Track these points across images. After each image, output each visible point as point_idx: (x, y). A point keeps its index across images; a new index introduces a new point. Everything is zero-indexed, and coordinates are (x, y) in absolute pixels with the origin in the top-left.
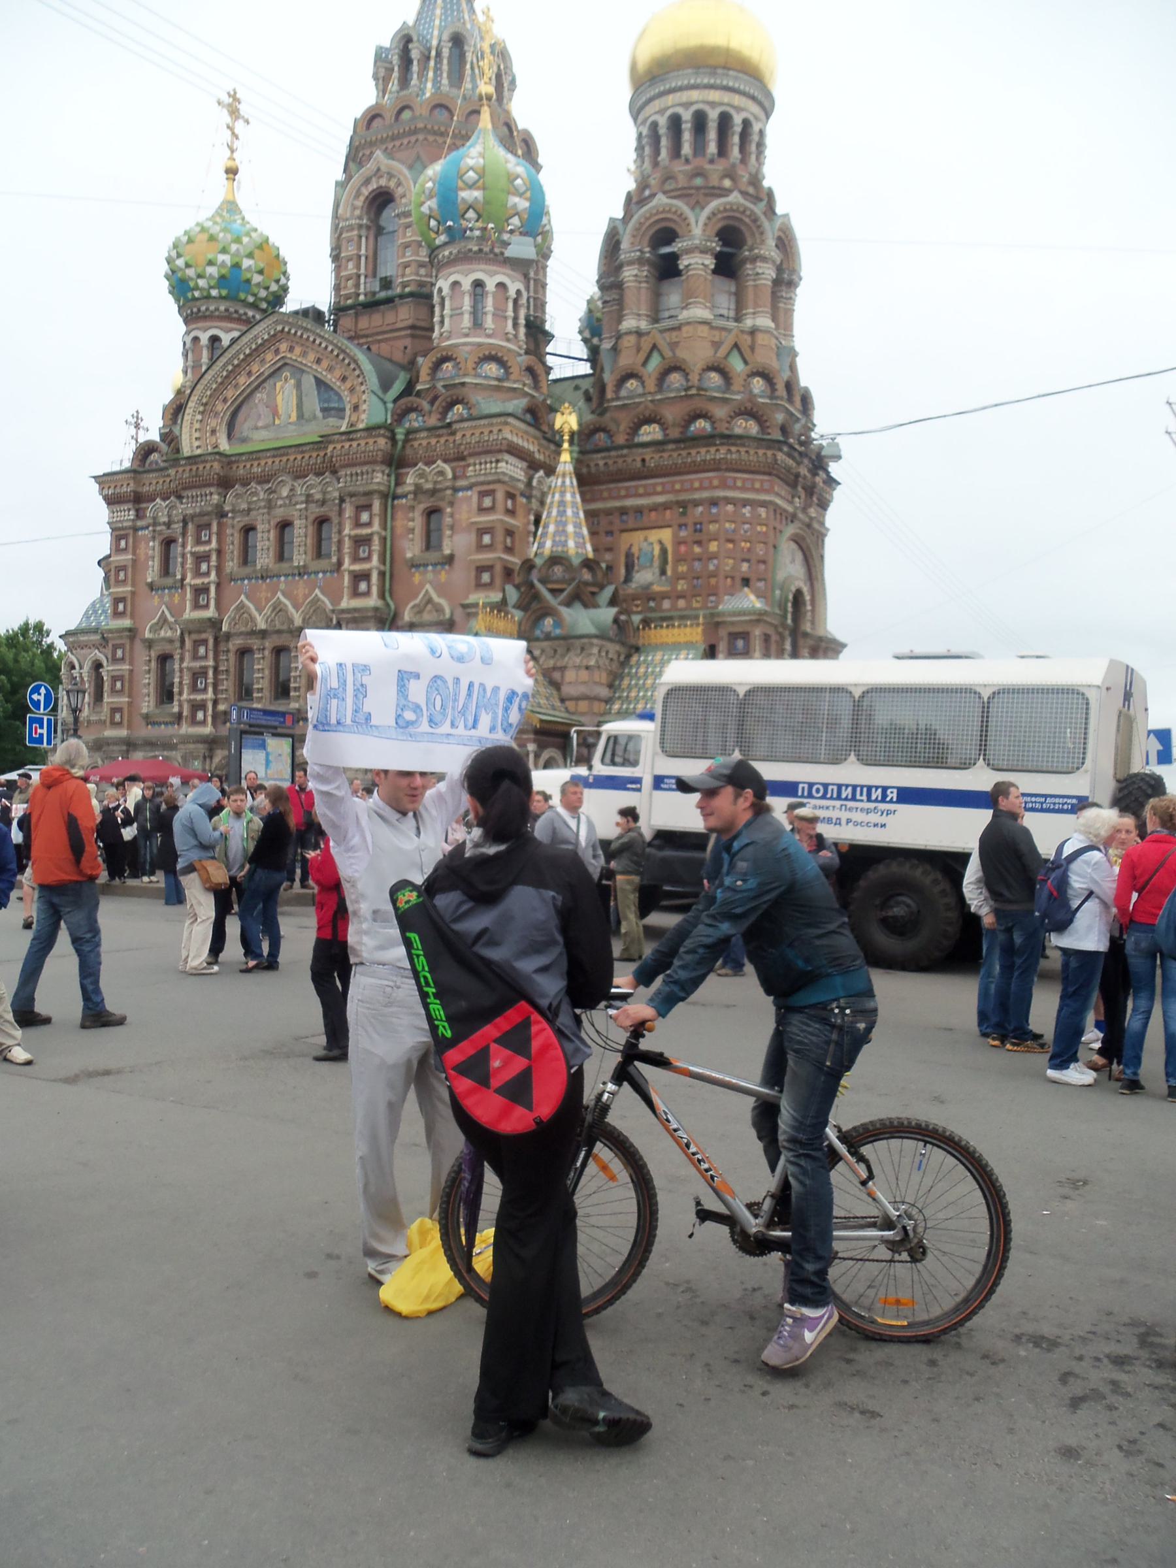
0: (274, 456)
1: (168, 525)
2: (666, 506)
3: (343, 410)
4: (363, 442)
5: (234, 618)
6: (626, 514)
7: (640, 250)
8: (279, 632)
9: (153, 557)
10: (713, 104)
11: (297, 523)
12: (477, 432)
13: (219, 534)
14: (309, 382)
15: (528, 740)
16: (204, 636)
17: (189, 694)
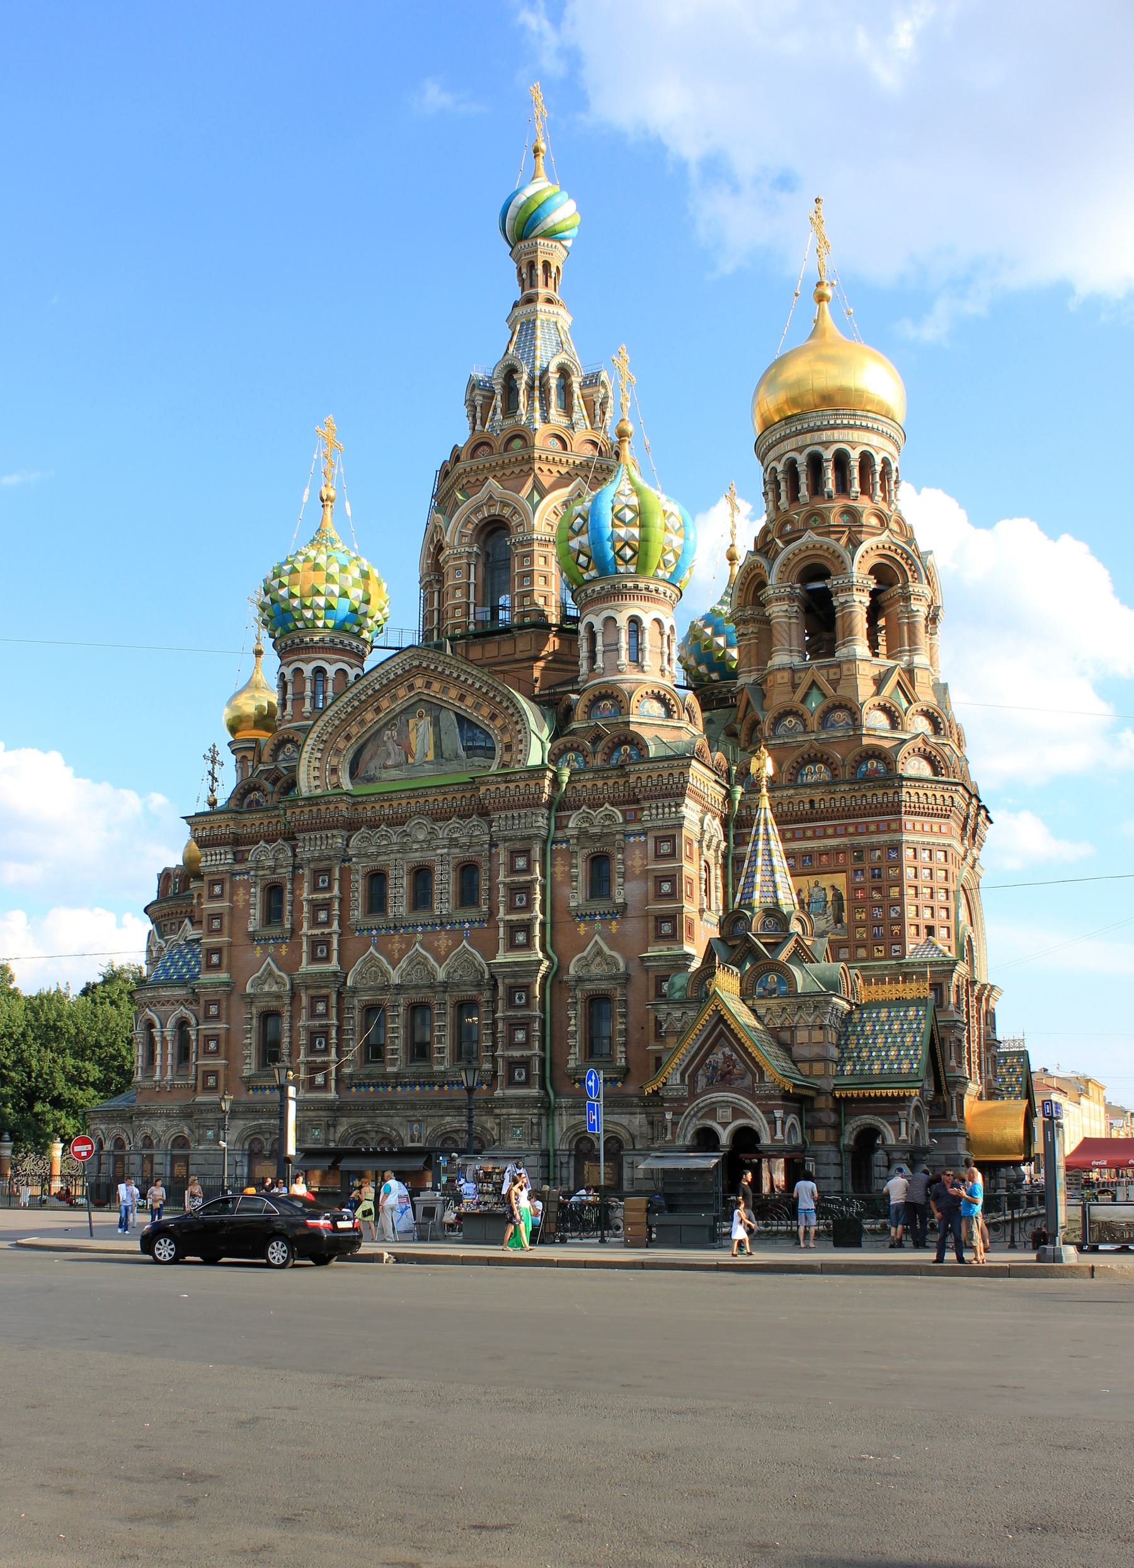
0: (409, 797)
1: (273, 870)
2: (837, 851)
3: (493, 749)
4: (522, 784)
5: (360, 973)
6: (793, 857)
7: (790, 586)
8: (416, 987)
11: (438, 869)
12: (654, 775)
13: (341, 880)
14: (448, 720)
15: (777, 1107)
16: (324, 991)
17: (307, 1055)
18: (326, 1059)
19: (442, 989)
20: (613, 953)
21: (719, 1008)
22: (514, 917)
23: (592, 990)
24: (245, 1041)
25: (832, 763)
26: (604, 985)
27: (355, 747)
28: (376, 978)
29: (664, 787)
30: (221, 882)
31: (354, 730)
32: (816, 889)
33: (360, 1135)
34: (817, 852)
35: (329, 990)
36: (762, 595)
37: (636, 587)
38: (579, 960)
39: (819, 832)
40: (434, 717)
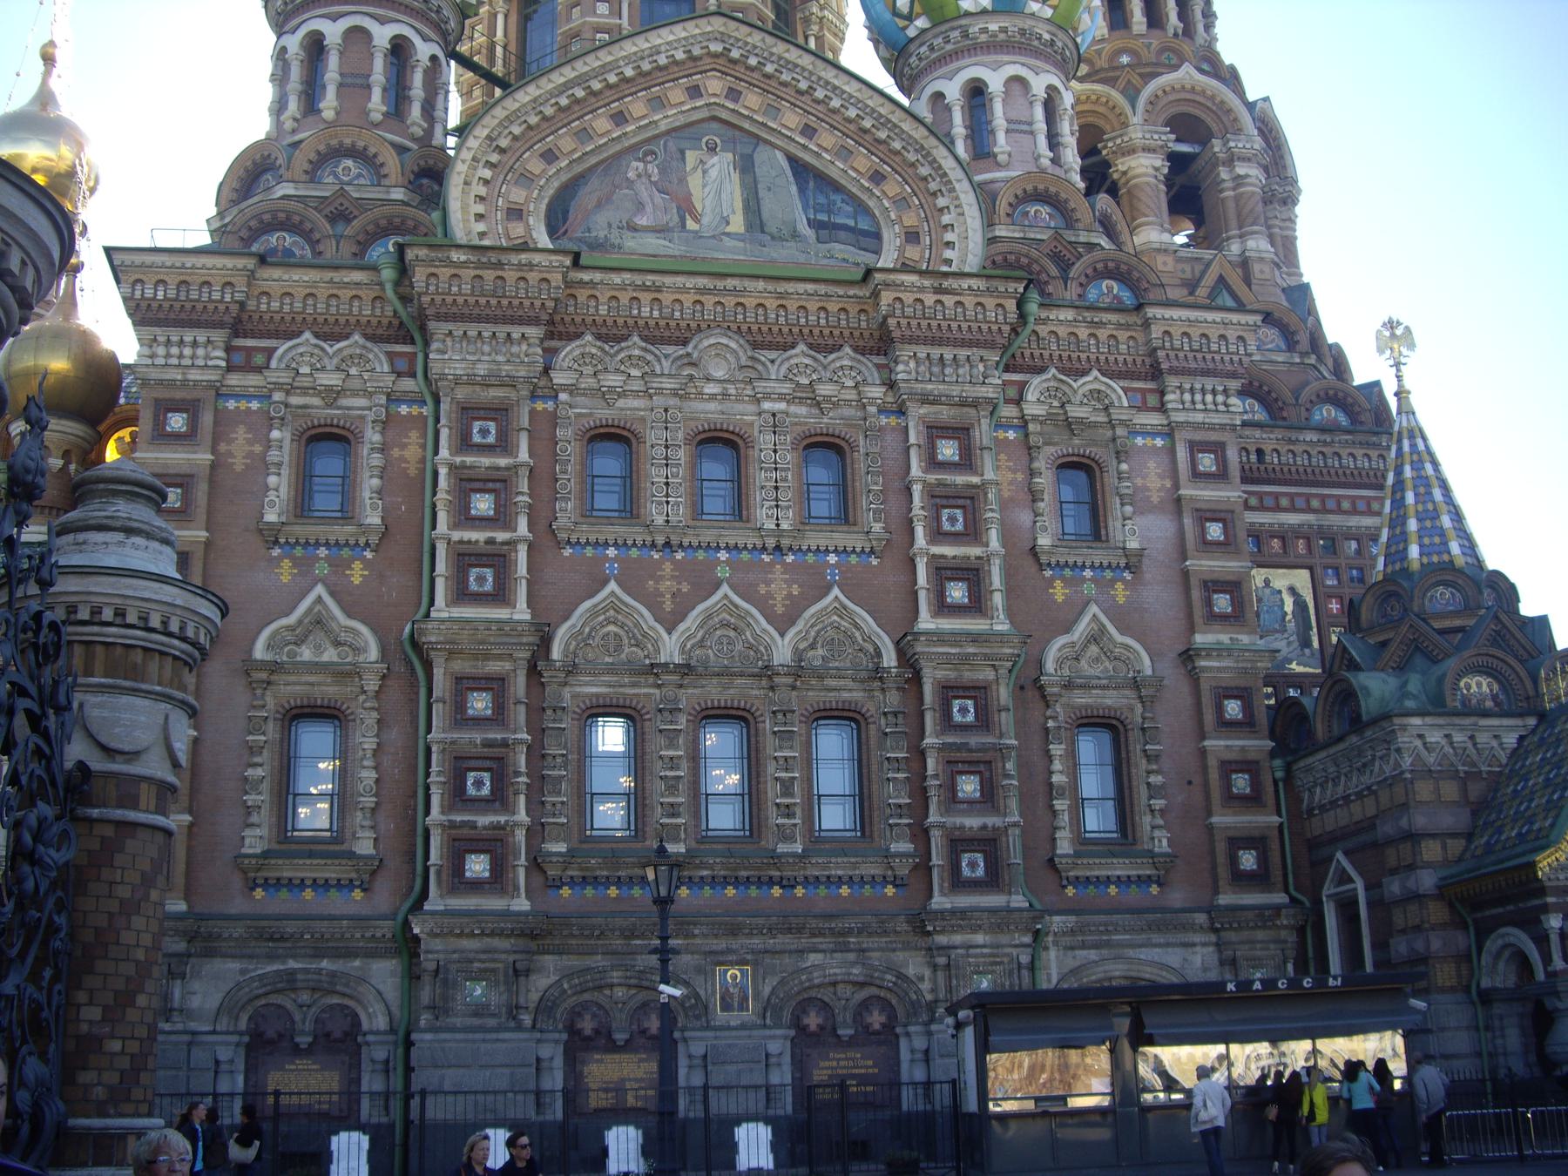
1: (332, 395)
3: (877, 236)
5: (580, 632)
8: (725, 673)
9: (279, 465)
14: (771, 165)
16: (494, 667)
18: (502, 819)
19: (790, 680)
22: (948, 551)
23: (1087, 707)
24: (250, 772)
25: (1276, 400)
26: (1111, 700)
27: (564, 177)
28: (619, 648)
30: (191, 408)
31: (566, 143)
32: (1267, 591)
33: (586, 996)
34: (1267, 531)
35: (508, 666)
36: (1110, 140)
38: (1059, 650)
39: (1269, 502)
40: (742, 156)
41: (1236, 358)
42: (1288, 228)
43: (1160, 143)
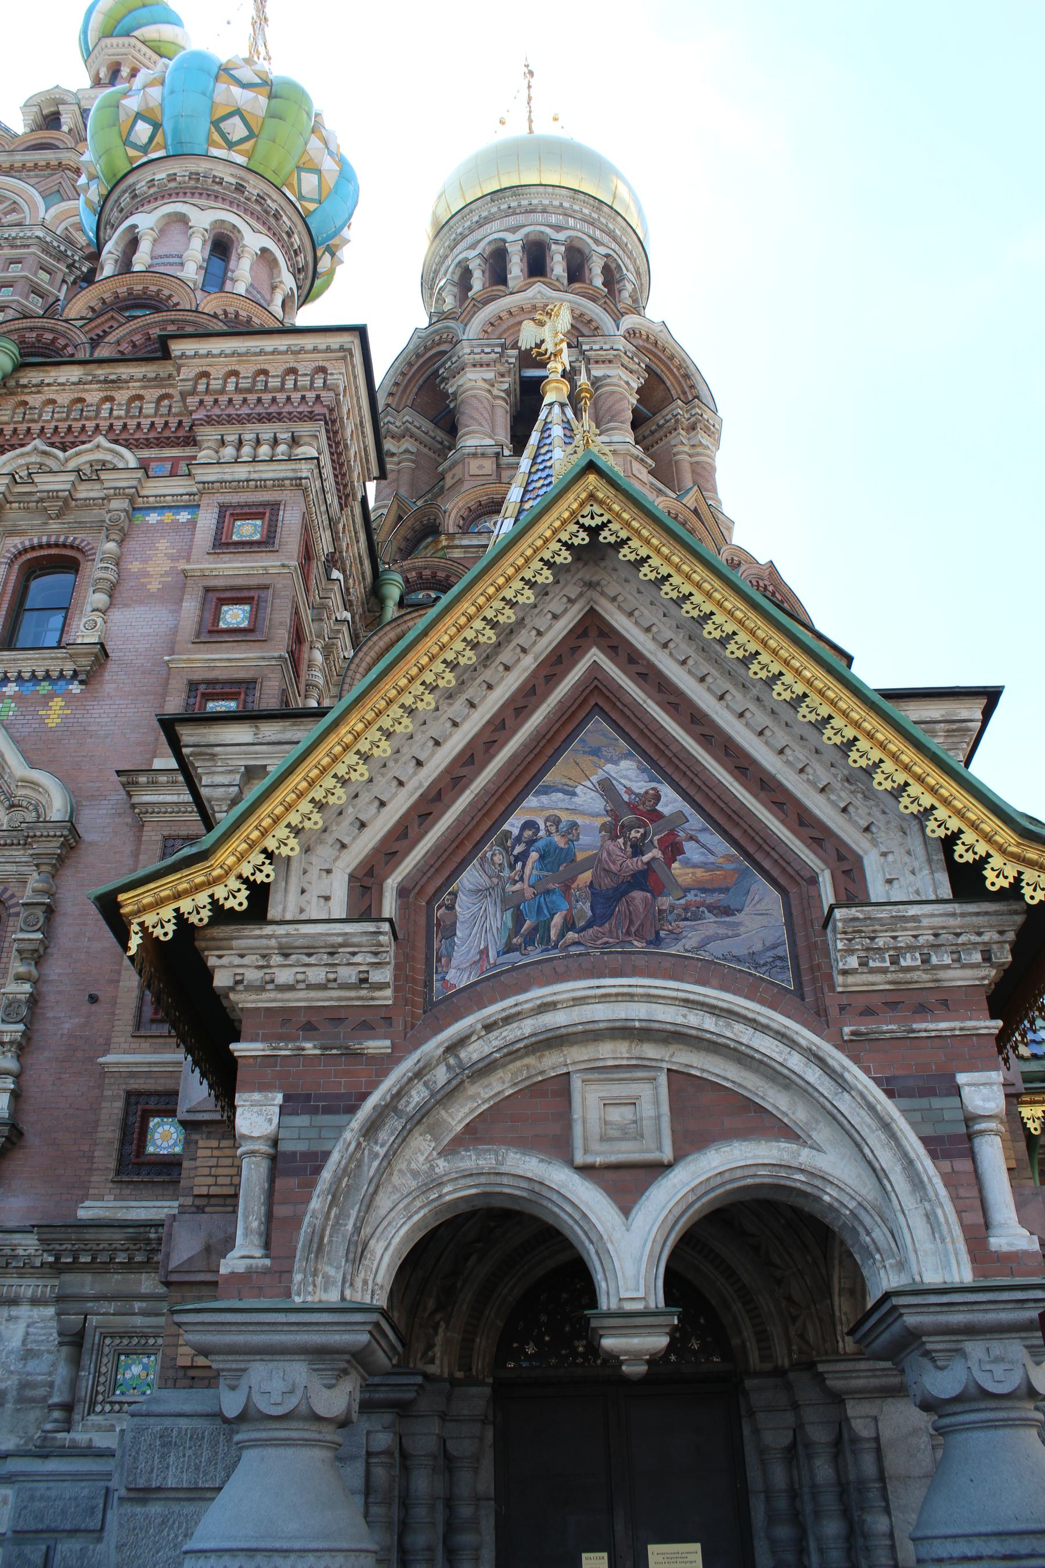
10: (596, 241)
12: (247, 370)
20: (37, 775)
21: (606, 537)
29: (267, 397)
37: (240, 188)
41: (311, 395)
42: (698, 454)
43: (493, 356)
